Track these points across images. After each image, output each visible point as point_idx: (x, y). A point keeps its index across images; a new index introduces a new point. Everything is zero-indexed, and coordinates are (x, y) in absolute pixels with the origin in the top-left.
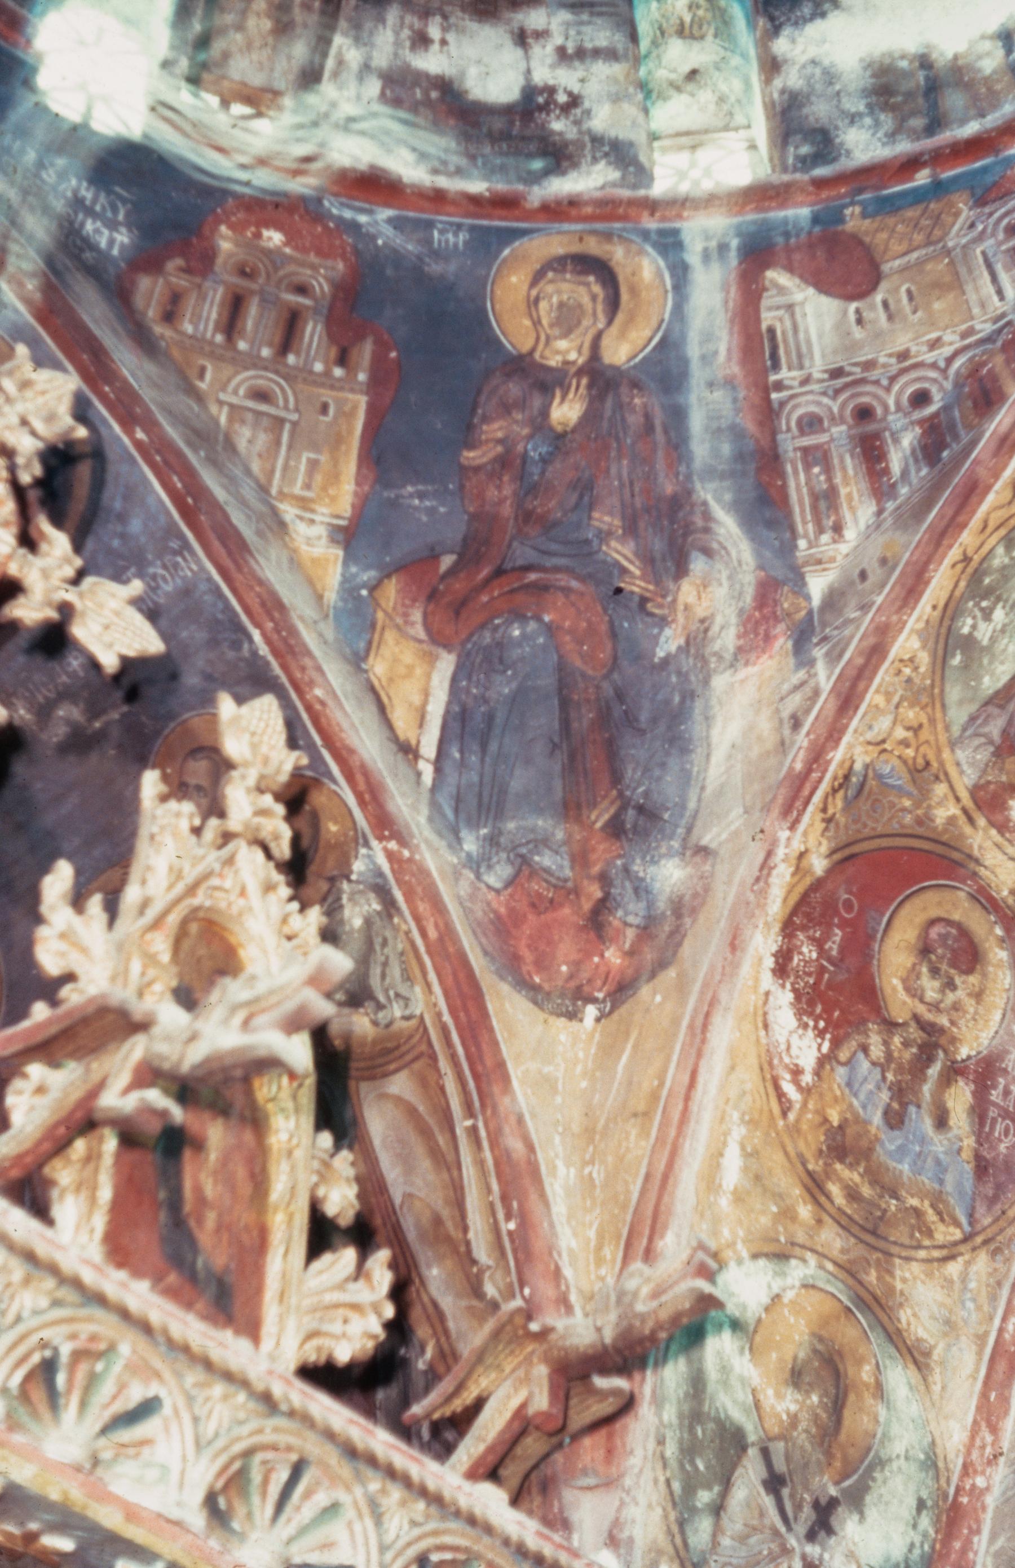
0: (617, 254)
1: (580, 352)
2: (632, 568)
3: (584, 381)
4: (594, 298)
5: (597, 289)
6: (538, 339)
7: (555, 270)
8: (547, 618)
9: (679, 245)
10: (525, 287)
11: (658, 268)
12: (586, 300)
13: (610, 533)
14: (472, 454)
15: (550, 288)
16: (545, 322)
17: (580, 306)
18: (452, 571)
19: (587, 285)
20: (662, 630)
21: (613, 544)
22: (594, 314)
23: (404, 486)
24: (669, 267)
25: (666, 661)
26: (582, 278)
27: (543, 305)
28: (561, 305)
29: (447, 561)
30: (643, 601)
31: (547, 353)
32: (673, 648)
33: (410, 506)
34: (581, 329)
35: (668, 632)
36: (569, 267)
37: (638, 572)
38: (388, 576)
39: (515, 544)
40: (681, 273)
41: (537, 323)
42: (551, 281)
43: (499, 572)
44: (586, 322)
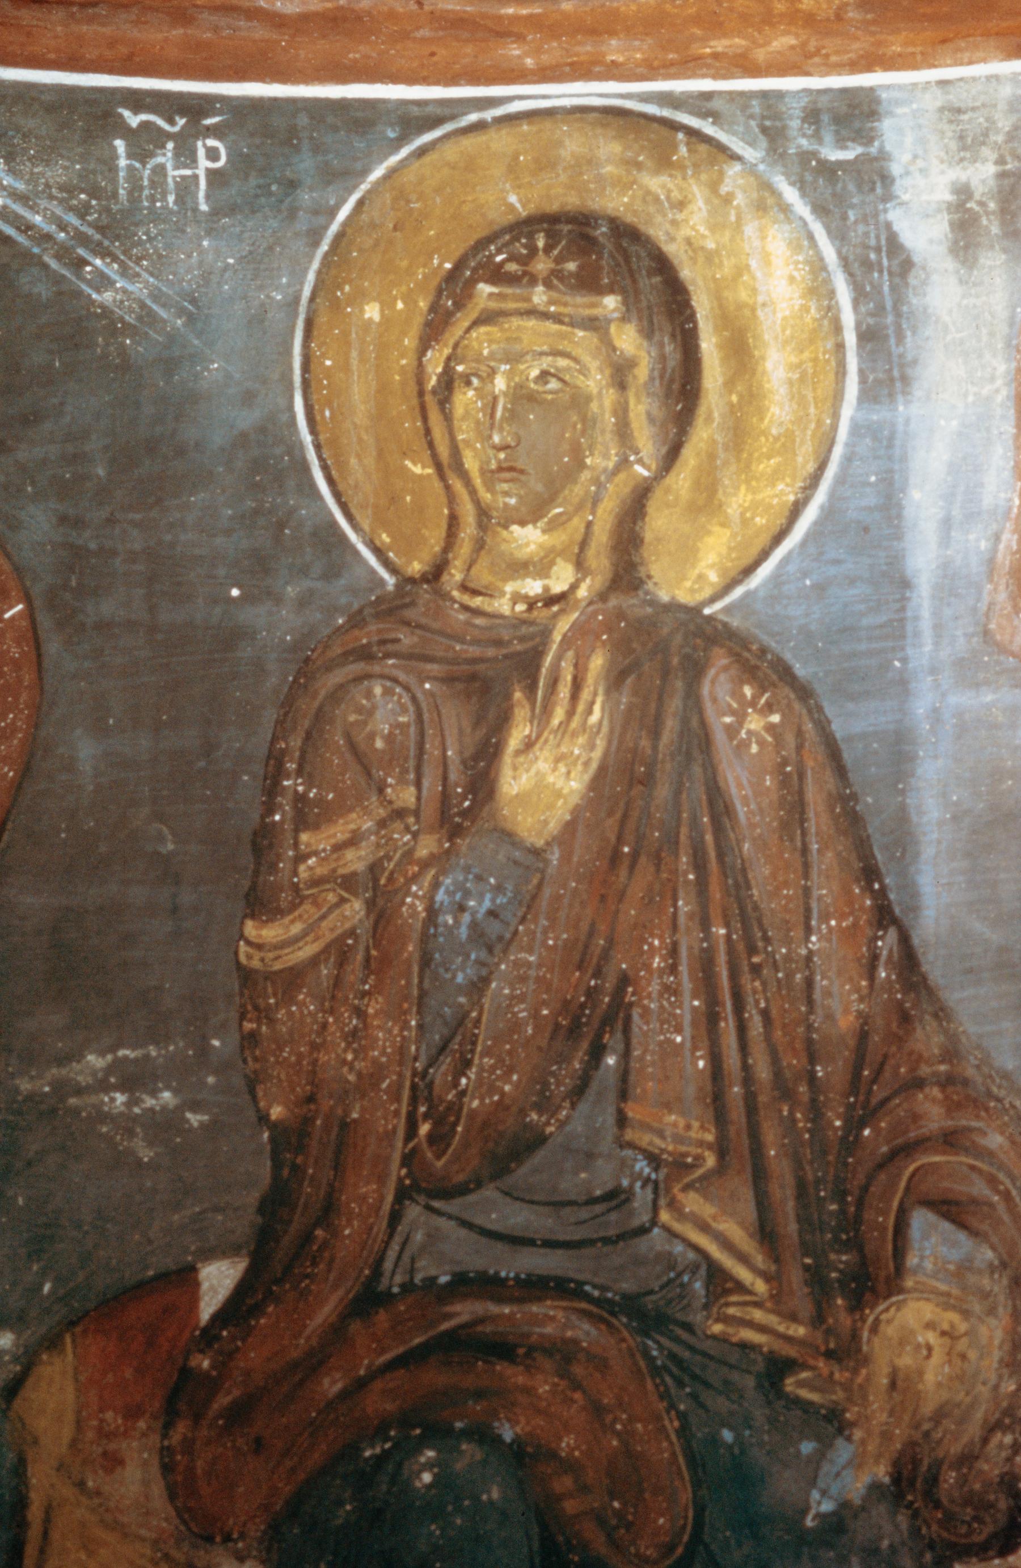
0: (685, 218)
1: (579, 564)
2: (743, 1274)
3: (597, 662)
4: (620, 374)
5: (628, 339)
6: (453, 522)
7: (497, 275)
8: (508, 1435)
9: (874, 177)
10: (409, 342)
11: (818, 266)
12: (595, 381)
13: (681, 1166)
14: (271, 933)
15: (484, 341)
16: (471, 463)
17: (579, 401)
18: (238, 1308)
19: (594, 324)
20: (826, 1445)
21: (692, 1202)
22: (623, 431)
23: (75, 1055)
24: (845, 263)
25: (836, 1525)
26: (579, 304)
27: (465, 399)
28: (522, 397)
29: (218, 1280)
30: (777, 1368)
31: (482, 575)
32: (855, 1487)
33: (103, 1117)
34: (577, 491)
35: (843, 1451)
36: (542, 265)
37: (761, 1287)
38: (52, 1343)
39: (413, 1211)
40: (882, 270)
41: (448, 466)
42: (487, 318)
43: (369, 1299)
44: (600, 460)
